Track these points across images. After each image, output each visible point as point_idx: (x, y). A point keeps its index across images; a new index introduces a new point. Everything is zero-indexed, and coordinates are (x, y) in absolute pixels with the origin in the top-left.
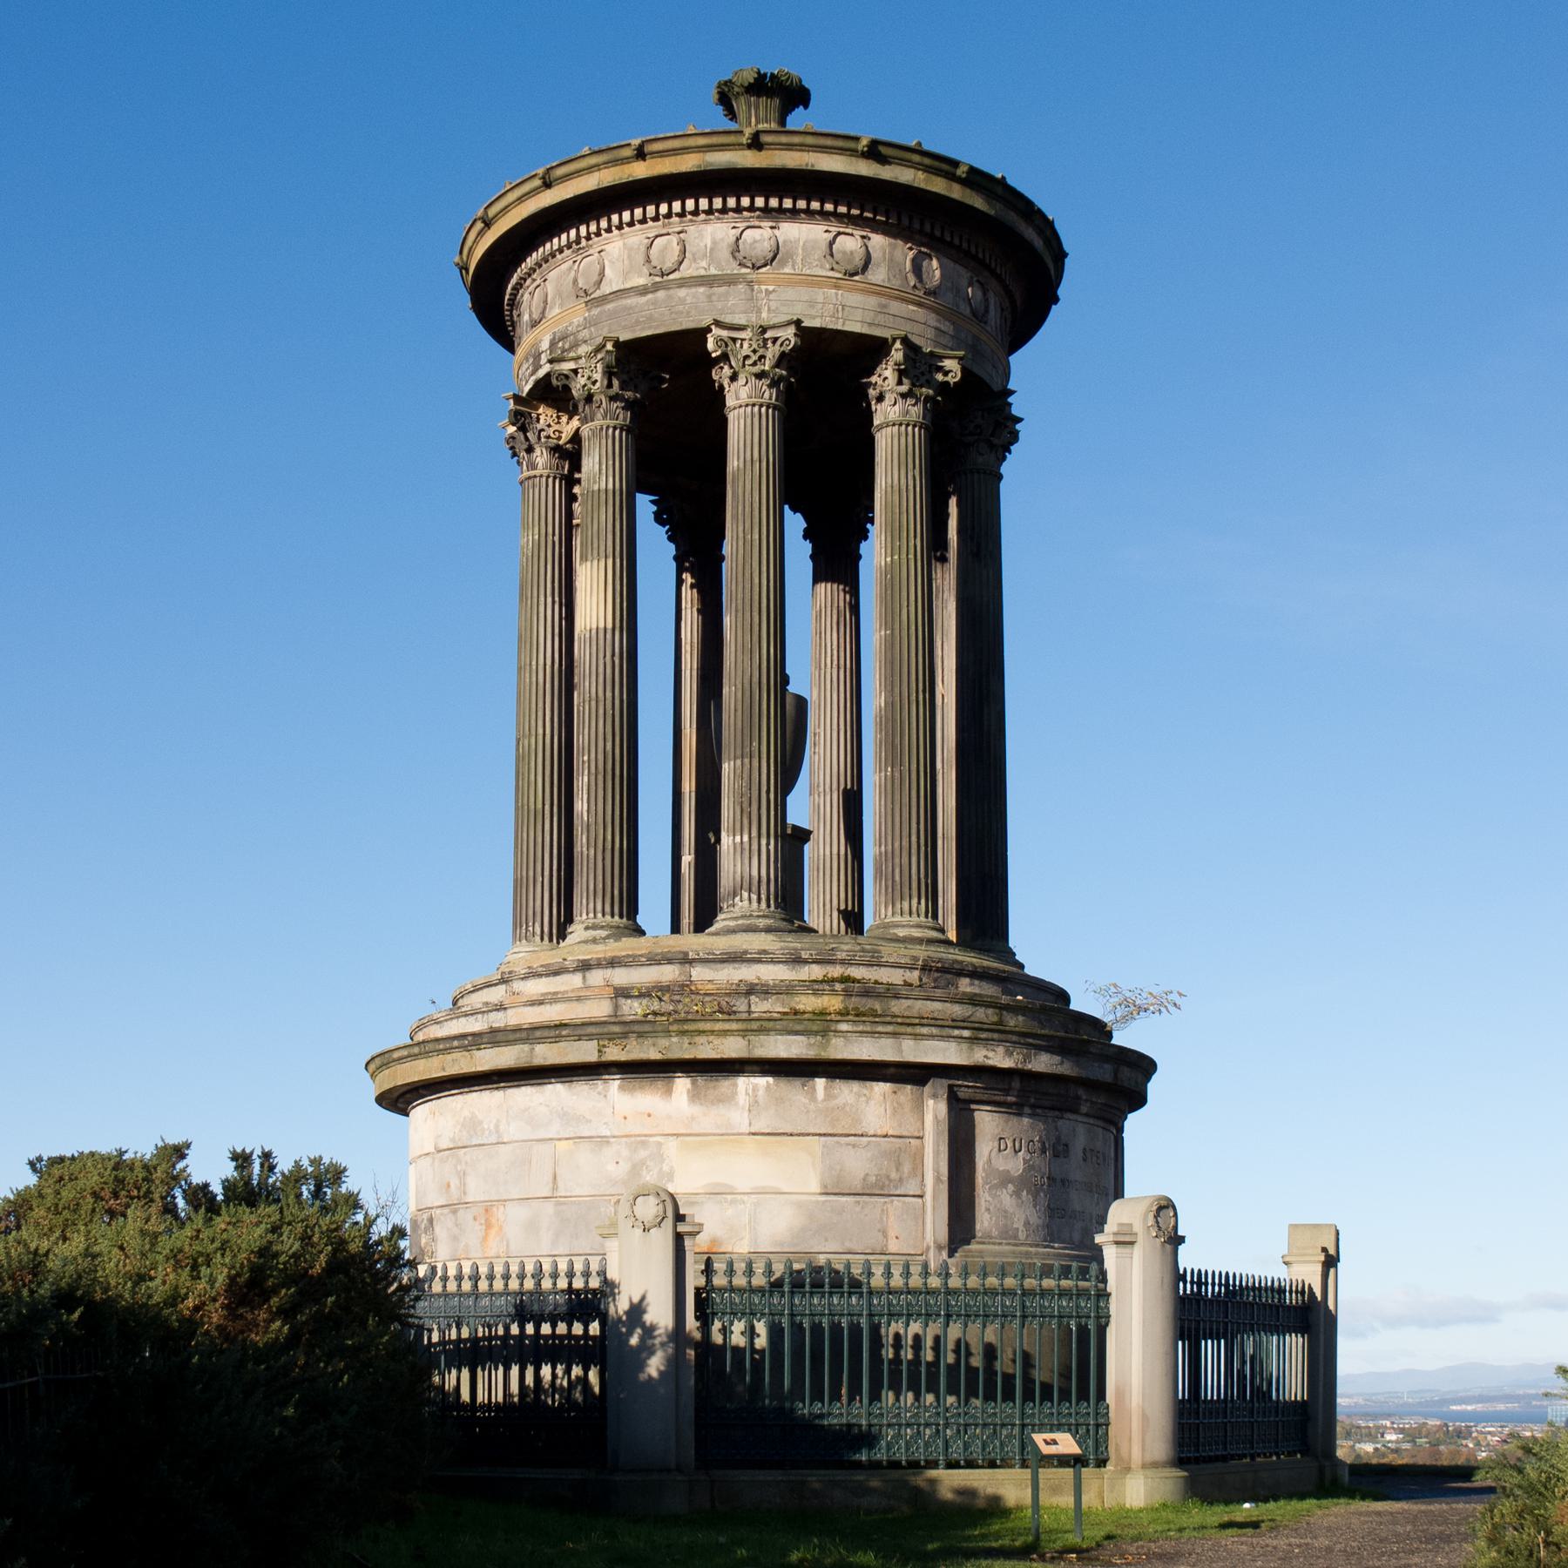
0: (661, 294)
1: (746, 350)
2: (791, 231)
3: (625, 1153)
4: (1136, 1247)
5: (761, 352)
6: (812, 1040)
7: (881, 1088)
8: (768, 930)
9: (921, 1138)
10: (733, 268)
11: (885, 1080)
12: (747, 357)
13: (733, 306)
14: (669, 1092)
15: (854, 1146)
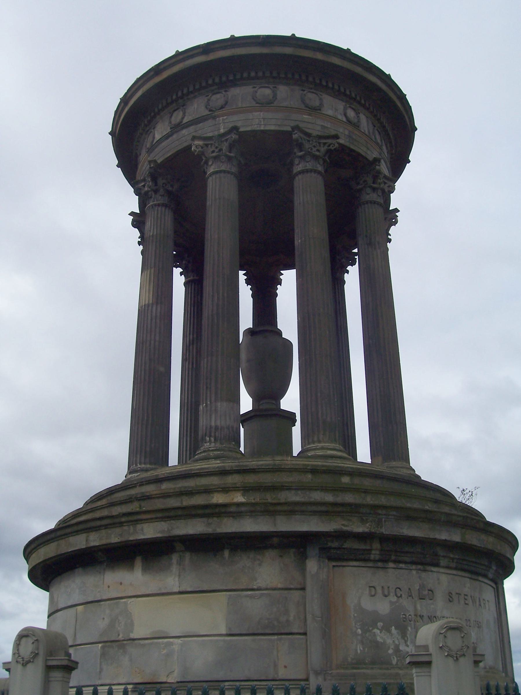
0: (175, 136)
1: (213, 148)
2: (235, 92)
3: (108, 611)
4: (434, 665)
5: (220, 147)
6: (210, 520)
7: (270, 554)
8: (216, 458)
9: (303, 589)
10: (207, 112)
11: (272, 547)
12: (213, 152)
13: (207, 129)
14: (131, 567)
15: (251, 597)
